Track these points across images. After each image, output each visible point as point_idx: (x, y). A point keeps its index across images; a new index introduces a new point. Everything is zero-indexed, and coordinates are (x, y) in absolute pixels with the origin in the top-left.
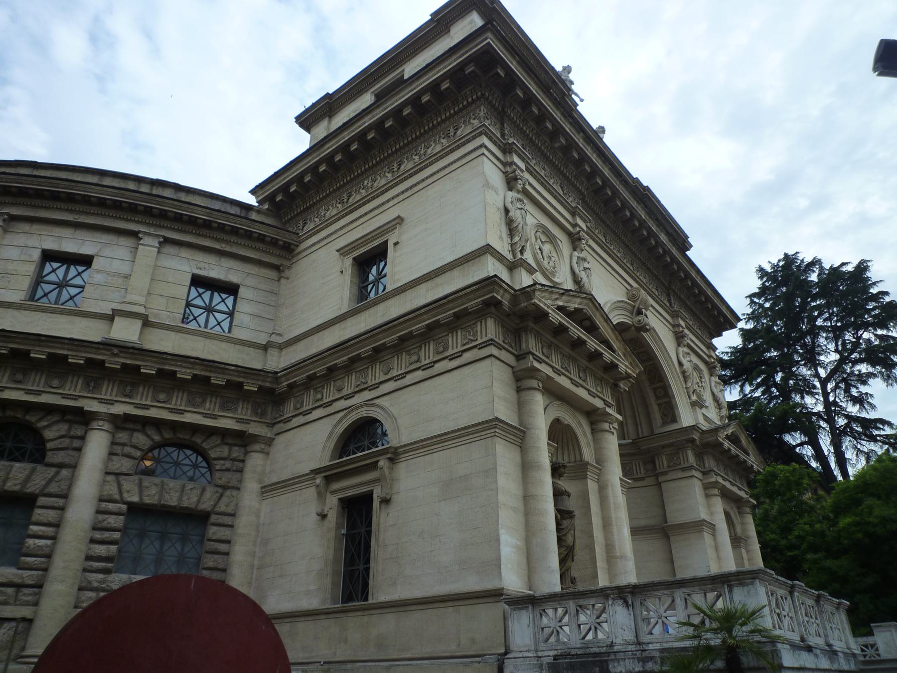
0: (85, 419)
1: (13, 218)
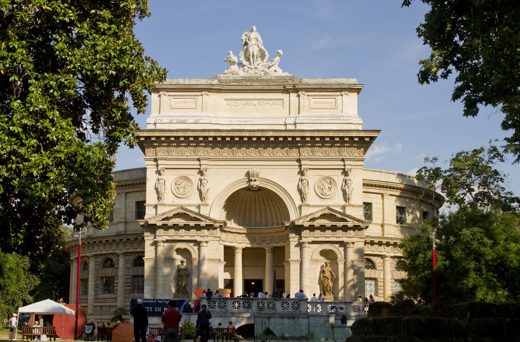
0: (118, 255)
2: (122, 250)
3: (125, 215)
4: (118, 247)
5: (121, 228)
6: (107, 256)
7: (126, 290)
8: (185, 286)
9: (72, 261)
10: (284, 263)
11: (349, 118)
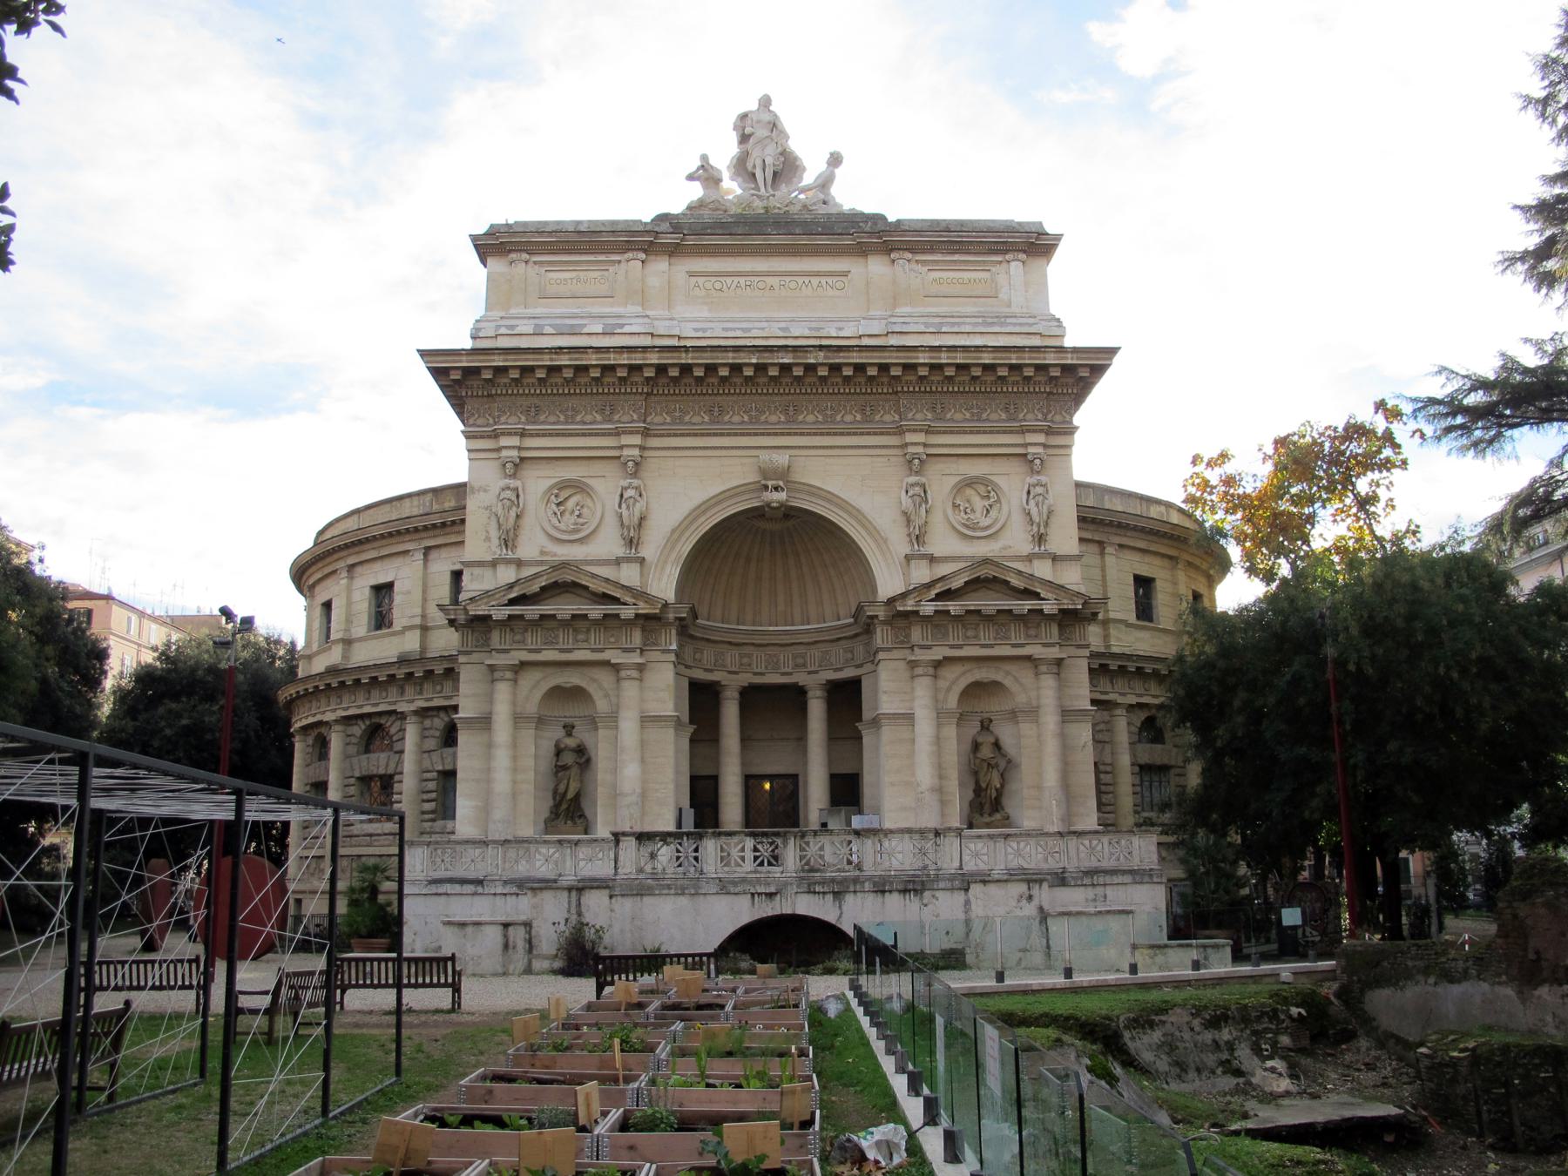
0: (402, 716)
1: (353, 566)
2: (412, 701)
3: (424, 608)
4: (402, 694)
5: (411, 643)
6: (376, 720)
7: (423, 813)
8: (578, 796)
9: (292, 735)
10: (860, 726)
11: (1031, 321)
